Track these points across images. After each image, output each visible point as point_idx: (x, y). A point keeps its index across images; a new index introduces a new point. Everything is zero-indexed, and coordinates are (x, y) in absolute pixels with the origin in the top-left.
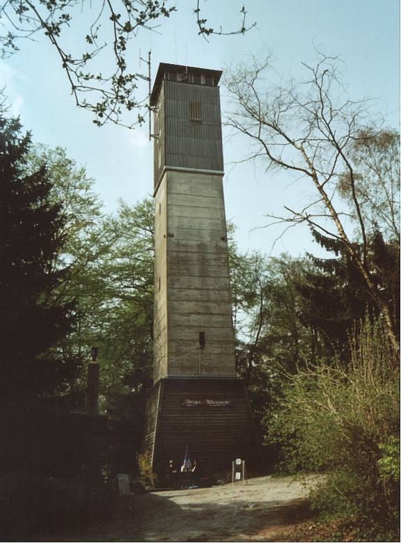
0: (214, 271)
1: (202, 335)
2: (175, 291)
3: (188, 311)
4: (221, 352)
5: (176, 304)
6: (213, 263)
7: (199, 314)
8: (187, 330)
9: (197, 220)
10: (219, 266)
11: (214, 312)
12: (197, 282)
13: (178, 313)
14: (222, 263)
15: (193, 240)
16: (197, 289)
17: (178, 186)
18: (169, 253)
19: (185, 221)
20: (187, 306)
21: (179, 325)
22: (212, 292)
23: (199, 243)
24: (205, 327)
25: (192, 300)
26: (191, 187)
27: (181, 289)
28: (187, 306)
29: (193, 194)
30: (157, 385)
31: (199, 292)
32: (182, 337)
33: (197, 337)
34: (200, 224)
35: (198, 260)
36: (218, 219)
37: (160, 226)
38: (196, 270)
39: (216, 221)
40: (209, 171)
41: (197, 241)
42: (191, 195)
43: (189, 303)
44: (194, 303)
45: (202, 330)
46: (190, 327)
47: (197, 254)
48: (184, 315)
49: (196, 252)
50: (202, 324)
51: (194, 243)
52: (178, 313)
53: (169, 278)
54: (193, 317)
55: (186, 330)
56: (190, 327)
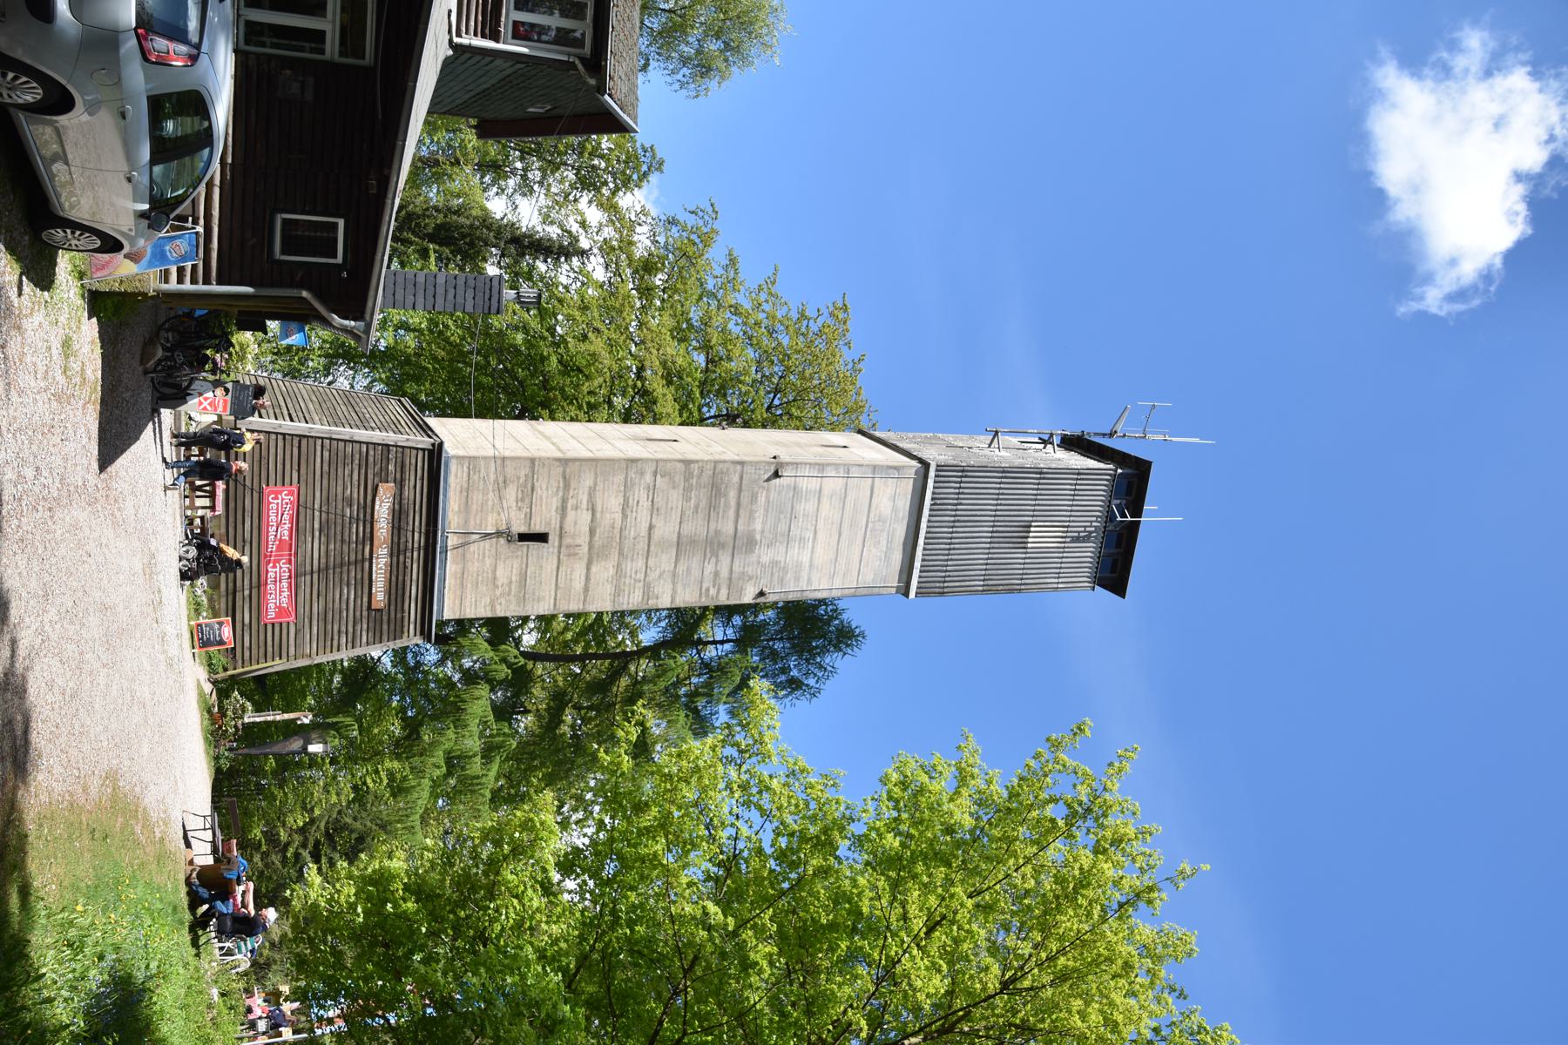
0: (689, 570)
1: (542, 538)
2: (648, 478)
3: (599, 509)
4: (499, 583)
5: (619, 478)
6: (709, 568)
7: (592, 532)
8: (555, 503)
9: (810, 535)
11: (594, 569)
12: (666, 529)
13: (595, 484)
14: (708, 590)
15: (764, 523)
16: (651, 527)
17: (889, 491)
18: (739, 467)
19: (807, 506)
20: (611, 502)
21: (567, 486)
22: (640, 564)
23: (758, 537)
24: (560, 546)
25: (625, 516)
26: (884, 522)
28: (611, 502)
29: (870, 525)
30: (426, 430)
31: (644, 533)
32: (538, 491)
33: (538, 528)
35: (717, 532)
36: (809, 580)
37: (798, 445)
38: (696, 527)
40: (917, 564)
41: (763, 532)
42: (867, 522)
43: (619, 509)
45: (553, 538)
46: (563, 510)
47: (731, 531)
48: (590, 494)
49: (736, 529)
50: (567, 541)
52: (595, 484)
53: (680, 466)
54: (587, 516)
55: (555, 499)
56: (563, 510)
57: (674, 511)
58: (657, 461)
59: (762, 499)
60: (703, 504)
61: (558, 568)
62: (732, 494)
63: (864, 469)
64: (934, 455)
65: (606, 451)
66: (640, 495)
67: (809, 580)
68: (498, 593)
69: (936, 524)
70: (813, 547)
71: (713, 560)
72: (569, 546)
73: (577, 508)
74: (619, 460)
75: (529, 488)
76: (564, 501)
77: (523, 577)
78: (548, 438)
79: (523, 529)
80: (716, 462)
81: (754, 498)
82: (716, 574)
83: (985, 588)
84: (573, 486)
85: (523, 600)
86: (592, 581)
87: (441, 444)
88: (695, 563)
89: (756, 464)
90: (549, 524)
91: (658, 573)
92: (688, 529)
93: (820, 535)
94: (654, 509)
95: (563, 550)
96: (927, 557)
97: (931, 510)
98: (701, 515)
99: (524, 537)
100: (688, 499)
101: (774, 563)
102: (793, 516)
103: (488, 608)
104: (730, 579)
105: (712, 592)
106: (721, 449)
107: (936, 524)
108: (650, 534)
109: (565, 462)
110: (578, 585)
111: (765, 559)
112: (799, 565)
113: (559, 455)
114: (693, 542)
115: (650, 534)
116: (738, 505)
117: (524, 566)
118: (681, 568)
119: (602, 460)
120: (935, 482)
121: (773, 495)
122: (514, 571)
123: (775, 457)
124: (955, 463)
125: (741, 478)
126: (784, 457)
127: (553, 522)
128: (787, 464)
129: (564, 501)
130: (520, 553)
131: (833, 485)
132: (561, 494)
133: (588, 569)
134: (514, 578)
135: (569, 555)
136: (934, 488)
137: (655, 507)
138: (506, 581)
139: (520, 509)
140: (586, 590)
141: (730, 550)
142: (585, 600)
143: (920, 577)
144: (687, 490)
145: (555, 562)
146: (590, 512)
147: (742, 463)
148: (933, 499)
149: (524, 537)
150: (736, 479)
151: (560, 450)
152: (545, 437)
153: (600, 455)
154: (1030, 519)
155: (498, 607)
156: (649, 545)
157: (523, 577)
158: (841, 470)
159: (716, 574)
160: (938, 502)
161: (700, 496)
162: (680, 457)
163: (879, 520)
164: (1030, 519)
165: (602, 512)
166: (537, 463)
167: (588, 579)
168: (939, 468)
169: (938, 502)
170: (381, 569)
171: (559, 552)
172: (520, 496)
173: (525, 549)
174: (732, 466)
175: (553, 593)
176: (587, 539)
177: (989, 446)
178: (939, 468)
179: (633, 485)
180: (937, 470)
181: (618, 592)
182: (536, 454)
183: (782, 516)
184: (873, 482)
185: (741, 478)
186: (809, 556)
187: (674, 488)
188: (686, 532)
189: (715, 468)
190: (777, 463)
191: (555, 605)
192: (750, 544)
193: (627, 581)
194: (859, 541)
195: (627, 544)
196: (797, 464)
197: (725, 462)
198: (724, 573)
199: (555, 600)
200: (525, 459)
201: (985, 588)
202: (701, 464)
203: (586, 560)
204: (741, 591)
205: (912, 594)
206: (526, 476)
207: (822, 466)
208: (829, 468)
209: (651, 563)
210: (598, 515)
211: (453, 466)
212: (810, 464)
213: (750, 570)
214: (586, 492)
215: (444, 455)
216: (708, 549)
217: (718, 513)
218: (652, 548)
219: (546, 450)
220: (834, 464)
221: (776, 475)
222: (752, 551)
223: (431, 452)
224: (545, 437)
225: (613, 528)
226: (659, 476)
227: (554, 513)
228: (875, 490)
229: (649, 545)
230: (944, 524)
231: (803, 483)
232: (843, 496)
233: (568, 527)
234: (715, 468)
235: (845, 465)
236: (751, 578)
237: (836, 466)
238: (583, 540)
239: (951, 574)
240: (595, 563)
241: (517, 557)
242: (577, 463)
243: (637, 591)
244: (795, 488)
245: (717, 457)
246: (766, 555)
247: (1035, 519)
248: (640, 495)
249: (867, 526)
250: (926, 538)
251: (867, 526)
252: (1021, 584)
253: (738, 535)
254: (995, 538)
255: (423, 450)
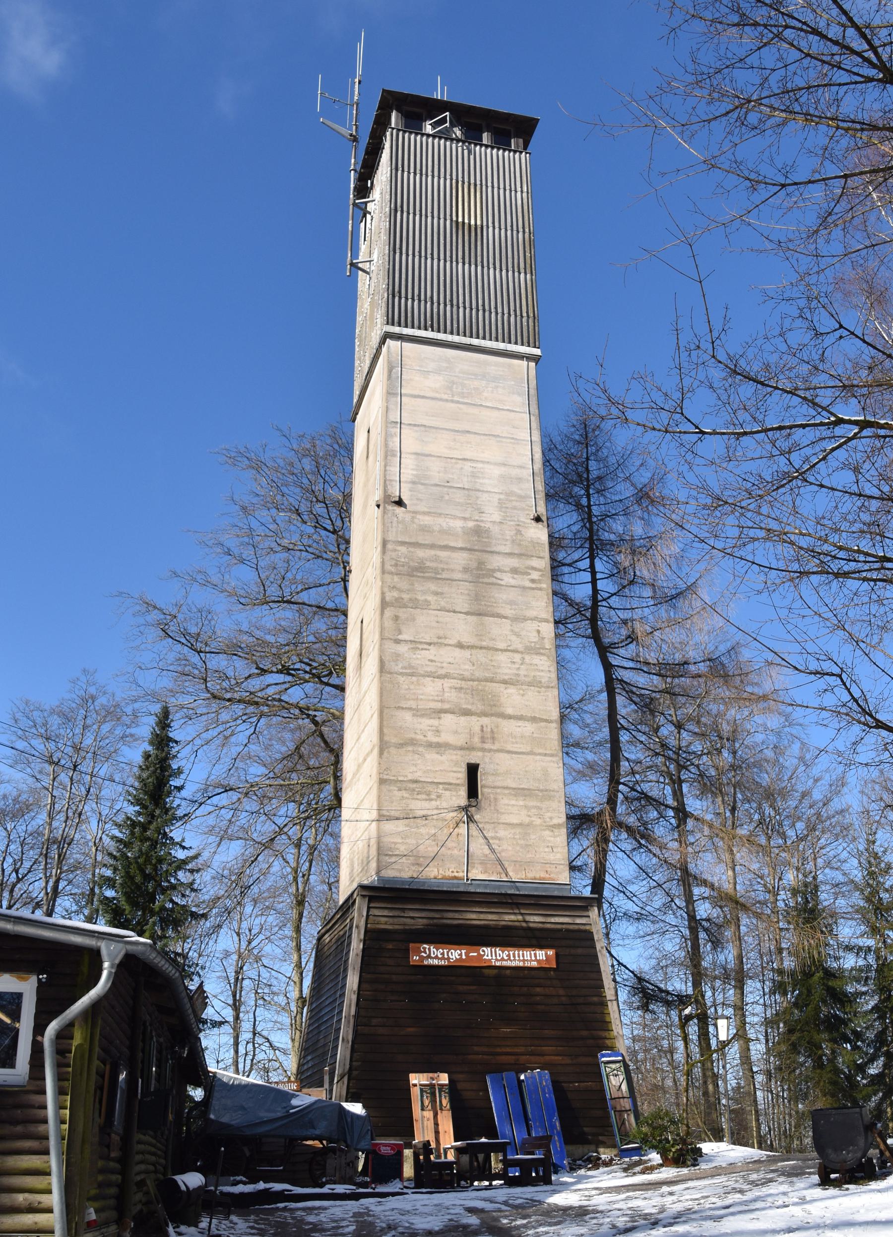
0: (512, 603)
1: (473, 771)
2: (403, 649)
3: (439, 705)
4: (527, 820)
6: (507, 579)
7: (467, 713)
8: (431, 756)
9: (467, 466)
10: (524, 588)
11: (510, 711)
14: (533, 581)
15: (455, 517)
16: (460, 646)
19: (435, 471)
21: (412, 742)
22: (502, 657)
23: (471, 524)
24: (483, 750)
26: (453, 383)
27: (415, 644)
29: (456, 398)
31: (467, 653)
32: (418, 775)
34: (474, 475)
35: (466, 570)
36: (521, 467)
39: (515, 472)
40: (501, 346)
41: (465, 519)
42: (452, 401)
43: (439, 683)
44: (454, 683)
46: (439, 747)
47: (465, 554)
48: (422, 716)
51: (458, 524)
52: (410, 709)
53: (389, 612)
55: (428, 756)
56: (439, 747)
57: (440, 619)
58: (382, 639)
59: (426, 520)
60: (433, 587)
61: (509, 752)
62: (421, 553)
63: (391, 406)
64: (379, 327)
65: (372, 699)
66: (421, 658)
67: (521, 467)
68: (538, 821)
69: (455, 325)
70: (482, 462)
71: (498, 575)
72: (483, 740)
73: (438, 731)
74: (382, 683)
75: (414, 785)
76: (430, 745)
77: (520, 792)
78: (359, 766)
79: (463, 792)
80: (383, 572)
81: (424, 529)
82: (515, 571)
83: (528, 271)
84: (413, 736)
85: (546, 794)
86: (524, 713)
87: (362, 887)
88: (502, 596)
89: (385, 529)
90: (456, 764)
91: (514, 638)
92: (461, 602)
93: (468, 455)
94: (439, 643)
95: (487, 746)
96: (494, 335)
97: (439, 331)
98: (446, 589)
99: (473, 791)
100: (427, 603)
101: (501, 505)
102: (447, 485)
103: (556, 832)
104: (520, 555)
105: (535, 575)
106: (370, 567)
107: (455, 325)
108: (468, 647)
109: (383, 746)
110: (528, 728)
111: (496, 517)
112: (503, 478)
113: (376, 751)
114: (477, 598)
115: (468, 647)
116: (432, 546)
117: (507, 792)
118: (508, 611)
119: (381, 701)
120: (406, 326)
121: (422, 508)
122: (513, 802)
123: (378, 506)
124: (384, 305)
125: (403, 543)
126: (377, 496)
127: (454, 757)
128: (385, 491)
129: (430, 745)
130: (492, 796)
131: (410, 441)
132: (421, 749)
133: (510, 717)
134: (521, 803)
135: (493, 738)
136: (413, 327)
137: (436, 640)
138: (524, 812)
139: (439, 797)
140: (534, 719)
141: (486, 556)
142: (546, 721)
143: (516, 343)
144: (415, 604)
145: (501, 755)
146: (442, 715)
147: (384, 543)
148: (426, 329)
149: (473, 791)
150: (403, 549)
151: (372, 750)
152: (358, 770)
153: (376, 705)
154: (448, 222)
155: (556, 821)
156: (481, 648)
157: (520, 792)
158: (393, 430)
159: (515, 571)
160: (429, 323)
161: (424, 590)
162: (378, 612)
163: (451, 388)
164: (448, 222)
165: (442, 701)
166: (385, 777)
167: (520, 718)
168: (390, 321)
169: (429, 323)
170: (509, 956)
171: (490, 751)
172: (424, 796)
173: (486, 790)
174: (389, 553)
175: (538, 757)
176: (474, 719)
177: (368, 273)
178: (390, 321)
179: (410, 667)
180: (393, 324)
181: (535, 683)
182: (375, 777)
183: (447, 497)
184: (406, 395)
185: (403, 543)
186: (492, 467)
187: (414, 620)
188: (466, 605)
189: (391, 573)
190: (385, 502)
191: (552, 755)
192: (478, 532)
193: (522, 672)
194: (475, 411)
195: (478, 674)
196: (385, 481)
197: (383, 563)
198: (513, 562)
199: (545, 755)
200: (379, 789)
201: (528, 271)
202: (386, 590)
203: (500, 720)
204: (535, 544)
205: (537, 352)
206: (400, 790)
207: (388, 454)
208: (391, 444)
209: (502, 645)
210: (446, 706)
211: (389, 873)
212: (385, 466)
213: (509, 534)
214: (420, 720)
215: (376, 884)
216: (486, 580)
217: (443, 570)
218: (484, 644)
219: (371, 766)
220: (386, 440)
221: (400, 503)
222: (487, 531)
223: (371, 899)
224: (358, 770)
225: (461, 688)
226: (400, 637)
227: (444, 758)
228: (416, 393)
229: (481, 648)
230: (455, 317)
231: (408, 473)
232: (423, 429)
233: (459, 741)
234: (391, 573)
235: (387, 427)
236: (519, 532)
237: (387, 437)
238: (475, 723)
239: (512, 308)
240: (502, 710)
241: (496, 799)
242: (385, 731)
243: (534, 662)
244: (414, 483)
245: (379, 571)
246: (492, 515)
247: (448, 217)
248: (421, 658)
249: (458, 402)
250: (471, 337)
251: (458, 402)
252: (524, 232)
253: (468, 546)
254: (471, 257)
255: (369, 908)
